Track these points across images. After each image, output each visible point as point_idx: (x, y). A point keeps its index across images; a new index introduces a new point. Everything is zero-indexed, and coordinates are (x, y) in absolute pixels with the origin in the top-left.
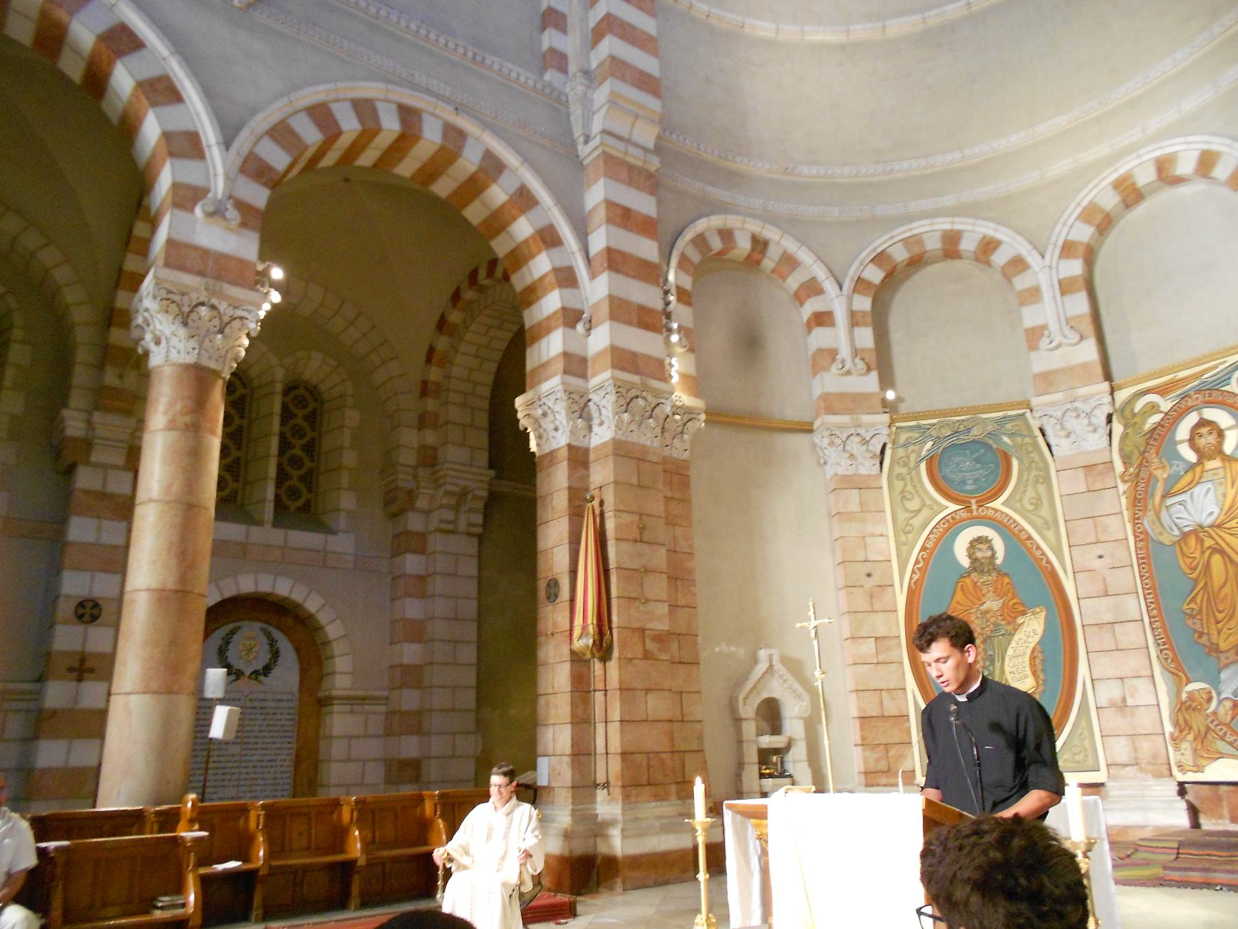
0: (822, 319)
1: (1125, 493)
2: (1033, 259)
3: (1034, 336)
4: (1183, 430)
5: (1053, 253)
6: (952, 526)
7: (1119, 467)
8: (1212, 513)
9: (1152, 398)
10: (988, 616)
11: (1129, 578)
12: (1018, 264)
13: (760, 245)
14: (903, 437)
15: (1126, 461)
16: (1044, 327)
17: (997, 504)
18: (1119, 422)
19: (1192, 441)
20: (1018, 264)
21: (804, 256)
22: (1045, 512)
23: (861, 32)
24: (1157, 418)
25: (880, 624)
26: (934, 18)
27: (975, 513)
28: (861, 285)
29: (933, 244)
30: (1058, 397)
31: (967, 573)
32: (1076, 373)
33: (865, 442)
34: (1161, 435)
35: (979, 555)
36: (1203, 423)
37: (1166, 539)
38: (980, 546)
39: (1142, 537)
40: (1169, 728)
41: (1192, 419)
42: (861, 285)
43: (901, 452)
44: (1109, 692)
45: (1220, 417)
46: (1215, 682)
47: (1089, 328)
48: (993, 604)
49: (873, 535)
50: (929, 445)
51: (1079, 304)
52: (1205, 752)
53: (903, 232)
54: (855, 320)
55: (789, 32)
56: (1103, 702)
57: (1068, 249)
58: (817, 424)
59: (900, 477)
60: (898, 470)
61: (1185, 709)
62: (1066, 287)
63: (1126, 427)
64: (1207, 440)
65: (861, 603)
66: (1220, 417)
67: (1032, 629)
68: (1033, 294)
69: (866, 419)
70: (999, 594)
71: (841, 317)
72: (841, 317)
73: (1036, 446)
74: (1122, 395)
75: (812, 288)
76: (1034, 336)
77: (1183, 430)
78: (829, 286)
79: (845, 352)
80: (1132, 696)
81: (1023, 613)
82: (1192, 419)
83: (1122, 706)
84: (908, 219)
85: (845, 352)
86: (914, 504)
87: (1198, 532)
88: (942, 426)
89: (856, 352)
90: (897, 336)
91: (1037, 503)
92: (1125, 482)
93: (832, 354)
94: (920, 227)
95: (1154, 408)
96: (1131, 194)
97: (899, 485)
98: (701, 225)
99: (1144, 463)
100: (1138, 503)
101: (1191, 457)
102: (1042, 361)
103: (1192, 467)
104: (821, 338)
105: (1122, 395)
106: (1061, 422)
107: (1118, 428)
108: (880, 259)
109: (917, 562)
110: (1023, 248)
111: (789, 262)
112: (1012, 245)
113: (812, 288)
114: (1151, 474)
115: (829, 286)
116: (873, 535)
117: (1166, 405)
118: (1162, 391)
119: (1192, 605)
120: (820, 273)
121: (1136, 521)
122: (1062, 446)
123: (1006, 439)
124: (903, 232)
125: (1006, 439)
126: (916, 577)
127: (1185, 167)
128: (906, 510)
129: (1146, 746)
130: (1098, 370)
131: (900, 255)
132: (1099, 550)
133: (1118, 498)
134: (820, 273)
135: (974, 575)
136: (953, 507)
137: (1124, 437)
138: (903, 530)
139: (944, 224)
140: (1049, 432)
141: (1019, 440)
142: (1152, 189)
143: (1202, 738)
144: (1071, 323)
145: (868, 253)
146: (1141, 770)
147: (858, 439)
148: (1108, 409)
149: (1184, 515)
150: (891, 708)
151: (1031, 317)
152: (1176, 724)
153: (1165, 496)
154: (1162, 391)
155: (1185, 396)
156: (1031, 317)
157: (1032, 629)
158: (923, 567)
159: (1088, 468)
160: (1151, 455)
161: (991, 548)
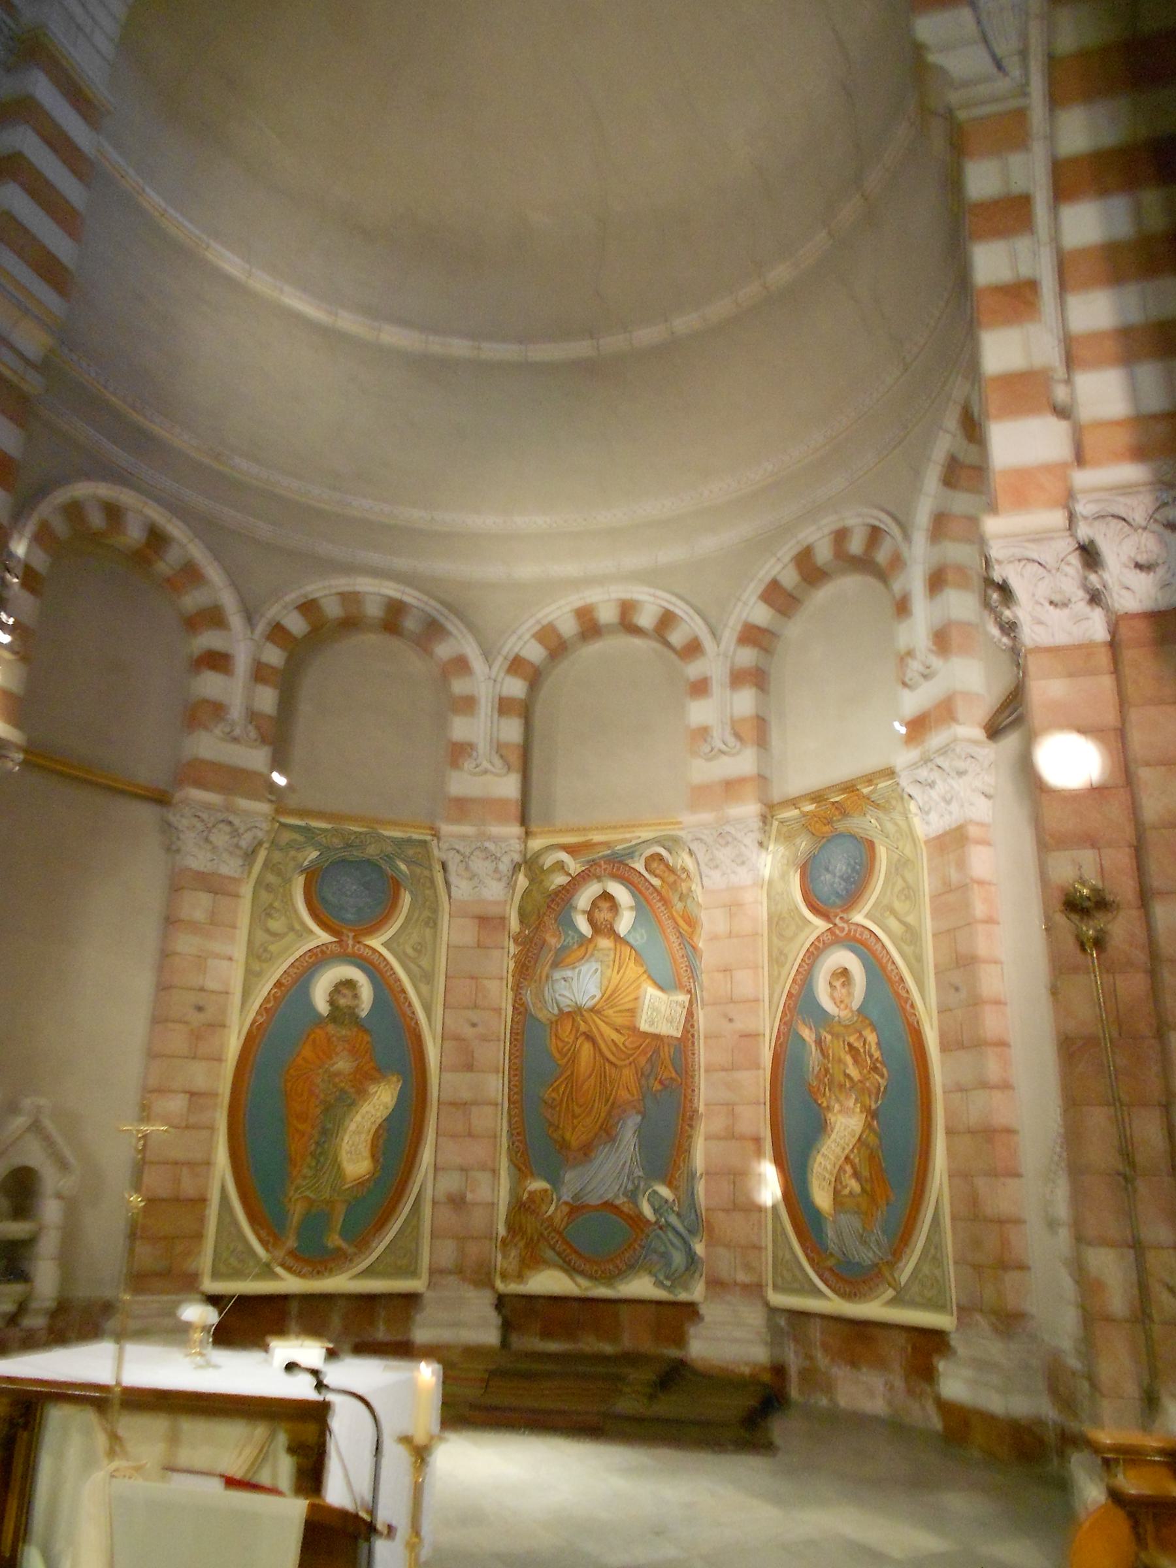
0: (218, 661)
1: (514, 956)
2: (477, 664)
3: (459, 752)
5: (499, 664)
6: (319, 959)
7: (514, 924)
8: (594, 996)
9: (563, 856)
10: (337, 1080)
11: (497, 1053)
13: (157, 539)
14: (286, 836)
15: (523, 916)
17: (375, 943)
18: (526, 876)
21: (213, 572)
22: (425, 962)
23: (349, 322)
24: (560, 880)
25: (198, 1075)
26: (436, 345)
27: (350, 950)
28: (278, 633)
29: (373, 610)
30: (467, 829)
32: (490, 807)
33: (235, 833)
34: (562, 898)
35: (342, 1002)
36: (606, 896)
37: (542, 1016)
38: (345, 991)
39: (520, 1008)
40: (502, 1231)
42: (278, 633)
43: (277, 856)
44: (450, 1183)
46: (555, 1181)
47: (515, 758)
48: (343, 1064)
49: (217, 956)
50: (315, 854)
51: (512, 731)
52: (531, 1261)
53: (343, 583)
54: (260, 673)
55: (262, 283)
56: (441, 1197)
57: (517, 665)
58: (178, 796)
59: (269, 888)
60: (271, 878)
61: (522, 1207)
62: (504, 706)
63: (532, 881)
64: (603, 915)
68: (467, 704)
69: (243, 803)
70: (353, 1052)
71: (242, 663)
72: (242, 663)
73: (432, 881)
74: (536, 844)
75: (214, 618)
76: (459, 752)
77: (585, 898)
78: (236, 620)
79: (236, 712)
80: (472, 1191)
81: (374, 1080)
83: (457, 1202)
84: (350, 569)
85: (236, 712)
87: (575, 1014)
88: (336, 832)
89: (253, 716)
90: (305, 708)
91: (419, 949)
92: (516, 941)
93: (218, 709)
94: (364, 584)
96: (590, 627)
97: (265, 896)
98: (82, 490)
99: (539, 927)
100: (525, 969)
102: (461, 784)
104: (210, 684)
105: (536, 844)
106: (465, 859)
107: (522, 881)
108: (308, 608)
109: (267, 1000)
111: (191, 574)
113: (214, 618)
114: (544, 941)
115: (236, 620)
116: (217, 956)
117: (574, 866)
118: (571, 849)
119: (554, 1095)
120: (228, 601)
121: (517, 989)
122: (462, 889)
123: (403, 867)
124: (343, 583)
125: (403, 867)
126: (261, 1020)
127: (646, 619)
128: (268, 931)
129: (473, 1249)
130: (515, 811)
131: (333, 610)
132: (474, 1016)
133: (504, 958)
134: (228, 601)
135: (331, 1029)
137: (527, 893)
138: (258, 956)
140: (452, 867)
141: (418, 870)
142: (610, 629)
143: (531, 1245)
144: (500, 748)
145: (293, 596)
146: (464, 1279)
147: (227, 829)
148: (517, 858)
149: (567, 993)
150: (188, 1187)
151: (461, 729)
152: (510, 1227)
154: (571, 849)
155: (593, 863)
156: (461, 729)
160: (549, 921)
161: (356, 996)
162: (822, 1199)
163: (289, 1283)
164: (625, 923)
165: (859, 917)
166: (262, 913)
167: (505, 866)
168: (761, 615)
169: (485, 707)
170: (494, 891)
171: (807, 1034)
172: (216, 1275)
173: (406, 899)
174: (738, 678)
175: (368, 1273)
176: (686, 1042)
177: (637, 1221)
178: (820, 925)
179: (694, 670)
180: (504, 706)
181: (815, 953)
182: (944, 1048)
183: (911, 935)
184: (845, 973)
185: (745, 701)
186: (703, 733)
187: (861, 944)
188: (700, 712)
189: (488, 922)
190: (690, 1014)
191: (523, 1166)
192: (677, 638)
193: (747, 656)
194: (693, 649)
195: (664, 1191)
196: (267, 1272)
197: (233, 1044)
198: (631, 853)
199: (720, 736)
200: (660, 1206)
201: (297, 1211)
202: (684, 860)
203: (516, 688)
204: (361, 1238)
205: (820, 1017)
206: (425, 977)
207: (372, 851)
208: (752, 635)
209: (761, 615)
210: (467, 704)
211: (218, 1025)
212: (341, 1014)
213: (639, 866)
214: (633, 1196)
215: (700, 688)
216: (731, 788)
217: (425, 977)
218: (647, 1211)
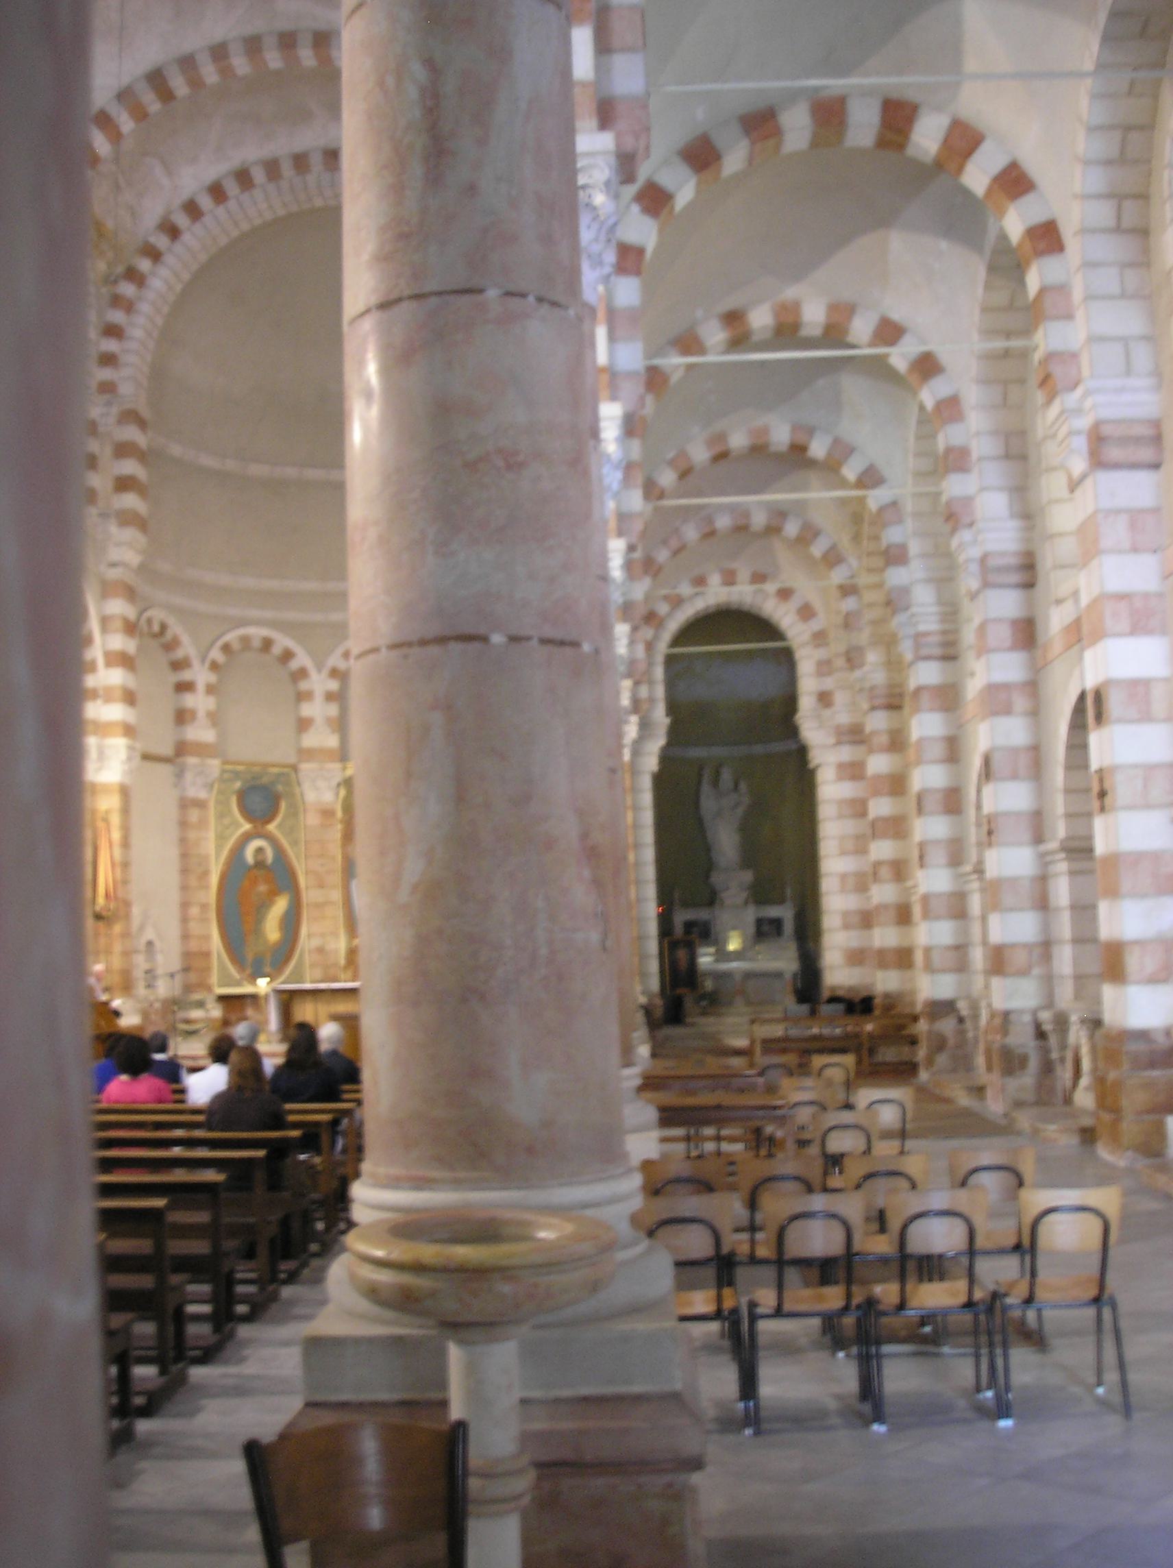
3: (304, 725)
5: (325, 672)
6: (247, 838)
12: (302, 673)
14: (226, 776)
17: (272, 827)
20: (302, 673)
21: (185, 639)
28: (214, 666)
31: (250, 868)
44: (315, 942)
51: (333, 710)
62: (330, 697)
67: (281, 905)
71: (201, 686)
83: (321, 950)
86: (226, 821)
94: (252, 631)
102: (311, 740)
112: (302, 659)
136: (247, 827)
138: (221, 838)
139: (264, 632)
151: (307, 710)
156: (307, 710)
157: (281, 905)
166: (220, 816)
167: (334, 782)
172: (220, 986)
173: (283, 805)
180: (330, 697)
189: (327, 813)
196: (239, 984)
197: (214, 879)
201: (250, 957)
203: (334, 685)
206: (295, 843)
207: (265, 780)
211: (206, 874)
212: (260, 864)
217: (295, 843)
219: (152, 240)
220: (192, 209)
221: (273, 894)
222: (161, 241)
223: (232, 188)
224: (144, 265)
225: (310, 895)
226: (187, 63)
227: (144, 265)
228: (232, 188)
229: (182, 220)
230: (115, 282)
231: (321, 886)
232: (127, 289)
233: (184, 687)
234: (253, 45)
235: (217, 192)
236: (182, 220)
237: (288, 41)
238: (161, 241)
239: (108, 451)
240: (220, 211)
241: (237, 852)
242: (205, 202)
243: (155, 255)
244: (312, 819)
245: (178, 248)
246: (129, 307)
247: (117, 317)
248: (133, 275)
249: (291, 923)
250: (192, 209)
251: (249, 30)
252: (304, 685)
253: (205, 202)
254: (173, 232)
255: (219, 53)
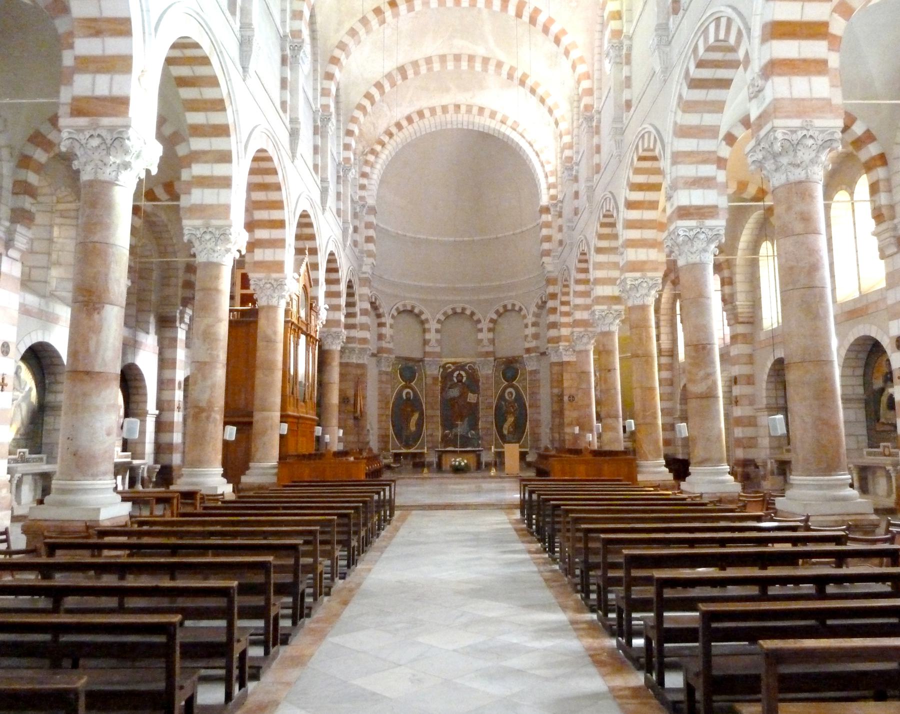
4: (455, 374)
5: (435, 321)
12: (427, 321)
15: (442, 377)
16: (430, 340)
19: (457, 377)
21: (383, 304)
24: (450, 370)
28: (393, 317)
40: (440, 440)
41: (457, 372)
44: (429, 432)
45: (463, 373)
46: (451, 432)
61: (444, 437)
62: (437, 331)
65: (384, 406)
66: (463, 373)
67: (416, 416)
71: (388, 325)
77: (455, 374)
82: (457, 372)
83: (431, 435)
87: (454, 399)
95: (449, 367)
100: (443, 390)
101: (455, 380)
103: (455, 383)
107: (441, 370)
108: (397, 309)
110: (429, 317)
117: (453, 368)
121: (441, 393)
133: (439, 387)
151: (427, 336)
153: (449, 388)
154: (453, 364)
155: (457, 367)
156: (427, 336)
157: (416, 416)
158: (396, 399)
159: (434, 378)
162: (505, 432)
163: (404, 451)
164: (464, 380)
165: (514, 383)
168: (495, 317)
169: (433, 331)
170: (436, 372)
171: (503, 403)
174: (490, 330)
175: (416, 449)
176: (477, 404)
177: (468, 438)
178: (506, 383)
179: (479, 326)
180: (437, 331)
181: (505, 388)
182: (530, 406)
183: (525, 388)
184: (511, 393)
185: (491, 335)
186: (481, 340)
187: (516, 389)
188: (480, 336)
189: (435, 379)
190: (478, 398)
191: (444, 427)
192: (475, 318)
193: (491, 325)
194: (479, 321)
195: (473, 432)
196: (400, 449)
198: (466, 365)
199: (485, 342)
200: (472, 435)
201: (404, 438)
202: (476, 367)
204: (416, 441)
205: (505, 400)
208: (492, 321)
209: (495, 317)
210: (429, 330)
212: (408, 399)
213: (467, 368)
214: (467, 433)
215: (481, 330)
216: (488, 354)
218: (470, 436)
219: (382, 138)
220: (399, 126)
221: (413, 411)
222: (386, 139)
223: (415, 118)
224: (378, 148)
225: (428, 412)
226: (415, 64)
227: (378, 148)
228: (415, 118)
229: (394, 130)
230: (366, 154)
231: (433, 409)
232: (371, 158)
233: (381, 325)
234: (443, 58)
235: (409, 119)
236: (394, 130)
237: (457, 58)
238: (386, 139)
239: (363, 225)
240: (410, 127)
241: (400, 393)
242: (404, 123)
243: (383, 144)
244: (429, 381)
245: (392, 141)
246: (372, 166)
247: (367, 169)
248: (373, 152)
249: (420, 424)
250: (399, 126)
251: (441, 52)
252: (427, 326)
253: (404, 123)
254: (391, 135)
255: (429, 61)
